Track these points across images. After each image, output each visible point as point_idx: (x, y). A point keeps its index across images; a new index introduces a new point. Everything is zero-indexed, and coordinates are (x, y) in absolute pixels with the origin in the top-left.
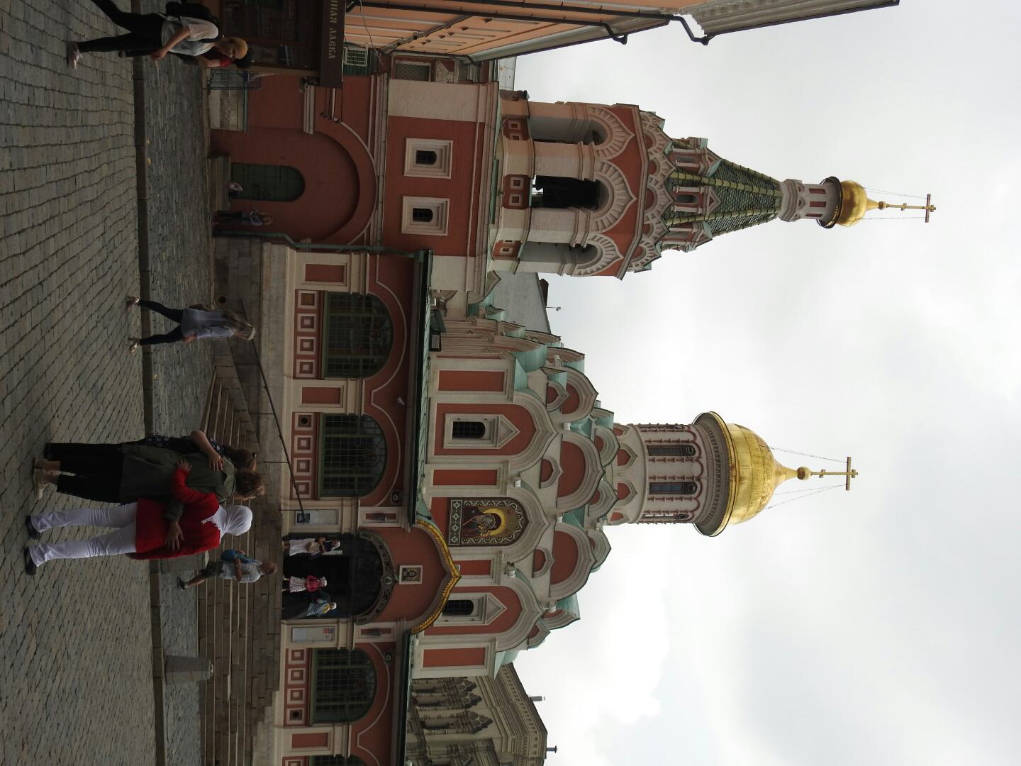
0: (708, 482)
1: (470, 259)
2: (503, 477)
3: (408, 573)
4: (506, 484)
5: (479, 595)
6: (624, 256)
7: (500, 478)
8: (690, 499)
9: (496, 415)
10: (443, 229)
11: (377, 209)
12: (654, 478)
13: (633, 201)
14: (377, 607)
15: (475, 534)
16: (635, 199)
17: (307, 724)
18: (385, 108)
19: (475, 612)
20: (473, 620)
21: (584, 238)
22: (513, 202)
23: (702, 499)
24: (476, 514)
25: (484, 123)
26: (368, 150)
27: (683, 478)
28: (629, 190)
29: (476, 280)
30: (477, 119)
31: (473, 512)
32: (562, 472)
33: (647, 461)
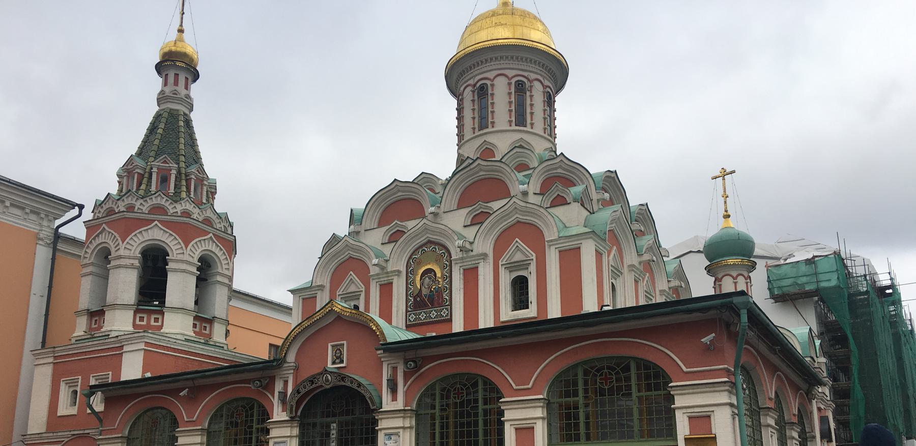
0: (476, 75)
1: (126, 349)
2: (383, 278)
3: (337, 358)
4: (387, 273)
5: (502, 271)
6: (155, 221)
7: (384, 280)
8: (492, 85)
9: (337, 296)
10: (107, 376)
11: (89, 434)
12: (474, 129)
14: (355, 386)
15: (439, 292)
18: (37, 436)
20: (530, 273)
22: (143, 321)
23: (491, 75)
24: (421, 296)
25: (55, 358)
27: (473, 101)
29: (136, 341)
30: (52, 363)
31: (418, 299)
32: (396, 221)
33: (465, 140)
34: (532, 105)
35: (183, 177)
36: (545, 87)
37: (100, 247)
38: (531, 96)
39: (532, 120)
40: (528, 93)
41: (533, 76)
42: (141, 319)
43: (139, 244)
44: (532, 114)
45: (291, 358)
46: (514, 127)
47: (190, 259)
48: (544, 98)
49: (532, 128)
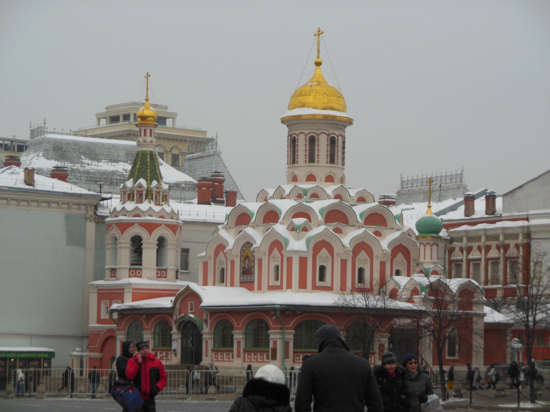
8: (298, 139)
13: (115, 226)
16: (114, 225)
17: (232, 351)
19: (278, 264)
21: (125, 243)
23: (297, 132)
25: (98, 290)
26: (103, 333)
28: (111, 228)
34: (318, 150)
35: (149, 193)
36: (328, 135)
37: (112, 236)
38: (318, 145)
39: (318, 159)
40: (316, 142)
41: (318, 132)
42: (132, 273)
43: (129, 236)
44: (318, 155)
45: (178, 306)
46: (308, 164)
47: (153, 241)
48: (328, 142)
49: (318, 163)
